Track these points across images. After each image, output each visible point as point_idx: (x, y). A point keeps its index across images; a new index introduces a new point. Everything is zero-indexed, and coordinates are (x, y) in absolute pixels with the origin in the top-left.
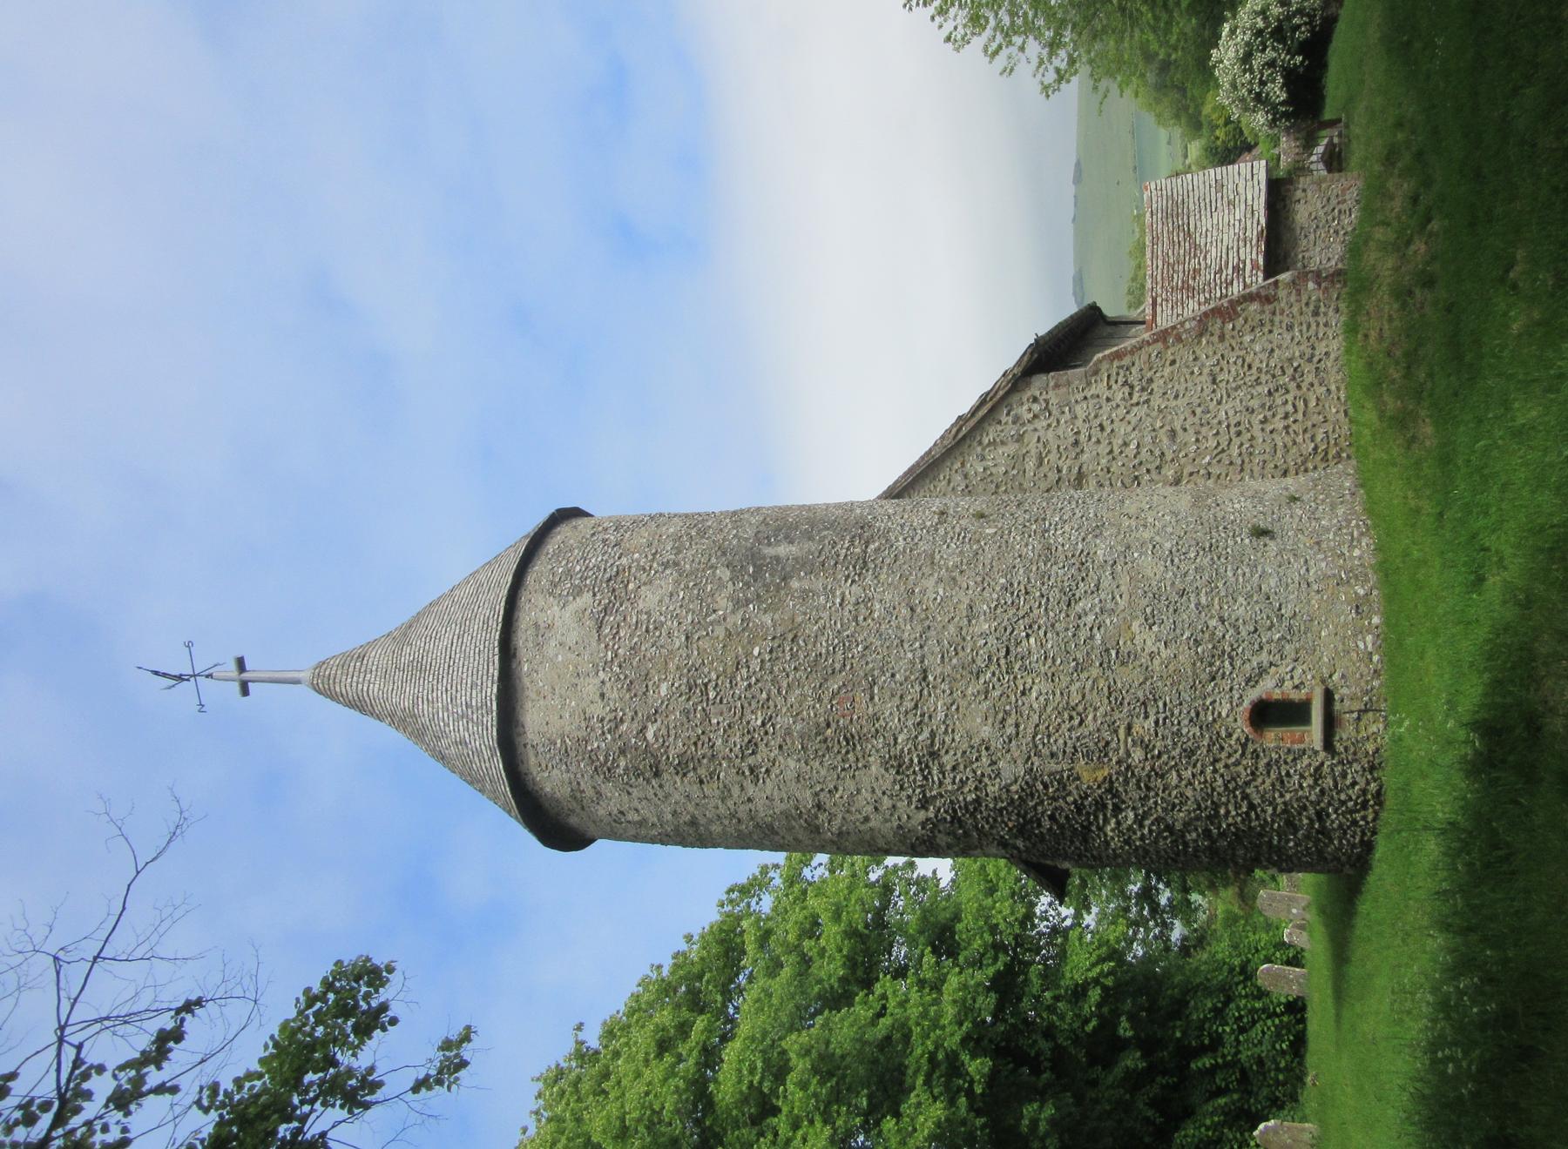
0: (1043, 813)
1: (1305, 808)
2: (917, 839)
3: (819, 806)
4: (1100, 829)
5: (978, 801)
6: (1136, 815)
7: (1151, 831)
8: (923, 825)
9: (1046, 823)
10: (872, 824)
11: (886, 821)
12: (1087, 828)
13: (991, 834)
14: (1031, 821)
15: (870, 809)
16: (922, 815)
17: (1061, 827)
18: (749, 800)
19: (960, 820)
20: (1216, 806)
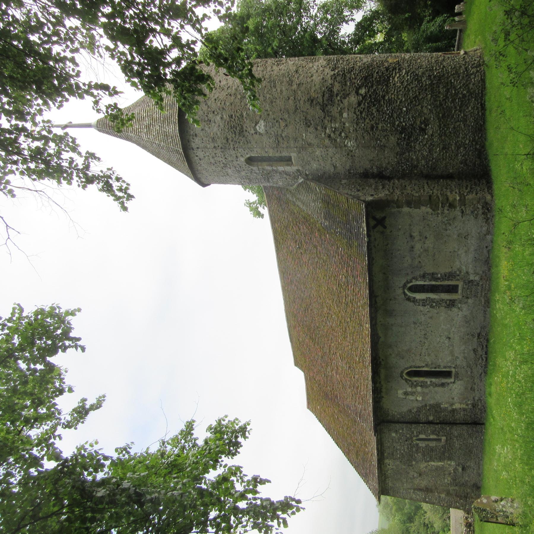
0: (375, 71)
1: (461, 67)
2: (327, 88)
3: (297, 71)
4: (394, 78)
5: (353, 67)
6: (406, 71)
7: (411, 77)
8: (332, 76)
9: (375, 75)
10: (314, 77)
11: (319, 76)
12: (389, 78)
13: (355, 83)
14: (370, 75)
15: (315, 71)
16: (332, 73)
17: (380, 77)
18: (272, 71)
19: (345, 75)
20: (433, 67)
